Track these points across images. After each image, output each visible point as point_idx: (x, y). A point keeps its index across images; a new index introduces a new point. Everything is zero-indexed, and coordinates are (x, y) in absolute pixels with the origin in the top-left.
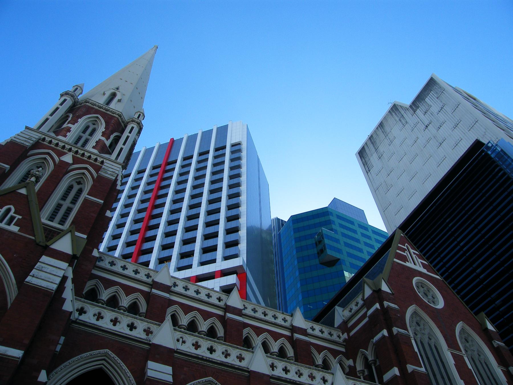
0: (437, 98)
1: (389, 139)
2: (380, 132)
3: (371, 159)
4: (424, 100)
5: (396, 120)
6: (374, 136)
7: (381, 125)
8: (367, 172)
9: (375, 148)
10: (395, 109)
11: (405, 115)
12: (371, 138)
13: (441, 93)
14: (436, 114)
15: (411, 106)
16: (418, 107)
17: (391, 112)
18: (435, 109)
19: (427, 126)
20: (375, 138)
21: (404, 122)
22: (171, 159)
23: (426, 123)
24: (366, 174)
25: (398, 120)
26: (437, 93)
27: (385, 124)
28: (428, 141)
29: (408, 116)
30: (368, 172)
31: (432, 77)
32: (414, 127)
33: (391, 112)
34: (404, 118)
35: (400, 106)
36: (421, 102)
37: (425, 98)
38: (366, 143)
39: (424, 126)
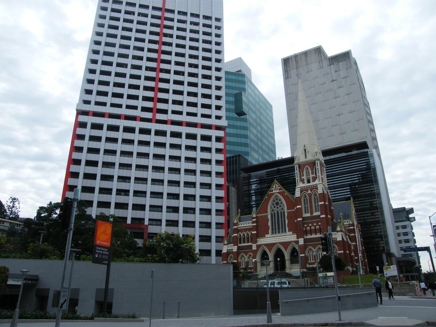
0: (346, 69)
1: (308, 69)
2: (303, 57)
3: (292, 71)
4: (339, 63)
5: (317, 60)
6: (299, 57)
7: (306, 54)
8: (286, 78)
9: (296, 66)
10: (319, 50)
11: (323, 61)
12: (296, 56)
13: (349, 67)
14: (341, 78)
15: (329, 59)
16: (333, 64)
17: (316, 51)
18: (342, 73)
19: (333, 81)
20: (299, 59)
21: (321, 66)
22: (167, 7)
23: (334, 79)
24: (285, 79)
25: (318, 60)
26: (347, 65)
27: (309, 55)
28: (331, 90)
29: (326, 63)
30: (287, 78)
31: (349, 52)
32: (325, 74)
33: (316, 51)
34: (322, 63)
35: (323, 52)
36: (336, 62)
37: (339, 62)
38: (291, 57)
39: (332, 80)
